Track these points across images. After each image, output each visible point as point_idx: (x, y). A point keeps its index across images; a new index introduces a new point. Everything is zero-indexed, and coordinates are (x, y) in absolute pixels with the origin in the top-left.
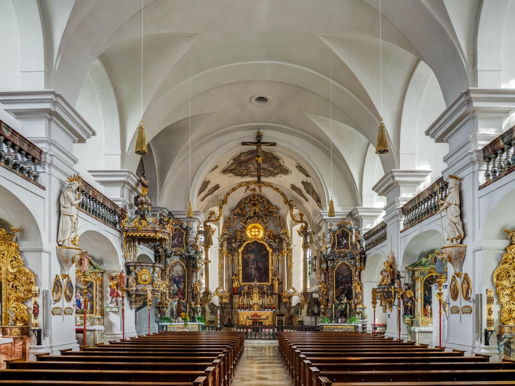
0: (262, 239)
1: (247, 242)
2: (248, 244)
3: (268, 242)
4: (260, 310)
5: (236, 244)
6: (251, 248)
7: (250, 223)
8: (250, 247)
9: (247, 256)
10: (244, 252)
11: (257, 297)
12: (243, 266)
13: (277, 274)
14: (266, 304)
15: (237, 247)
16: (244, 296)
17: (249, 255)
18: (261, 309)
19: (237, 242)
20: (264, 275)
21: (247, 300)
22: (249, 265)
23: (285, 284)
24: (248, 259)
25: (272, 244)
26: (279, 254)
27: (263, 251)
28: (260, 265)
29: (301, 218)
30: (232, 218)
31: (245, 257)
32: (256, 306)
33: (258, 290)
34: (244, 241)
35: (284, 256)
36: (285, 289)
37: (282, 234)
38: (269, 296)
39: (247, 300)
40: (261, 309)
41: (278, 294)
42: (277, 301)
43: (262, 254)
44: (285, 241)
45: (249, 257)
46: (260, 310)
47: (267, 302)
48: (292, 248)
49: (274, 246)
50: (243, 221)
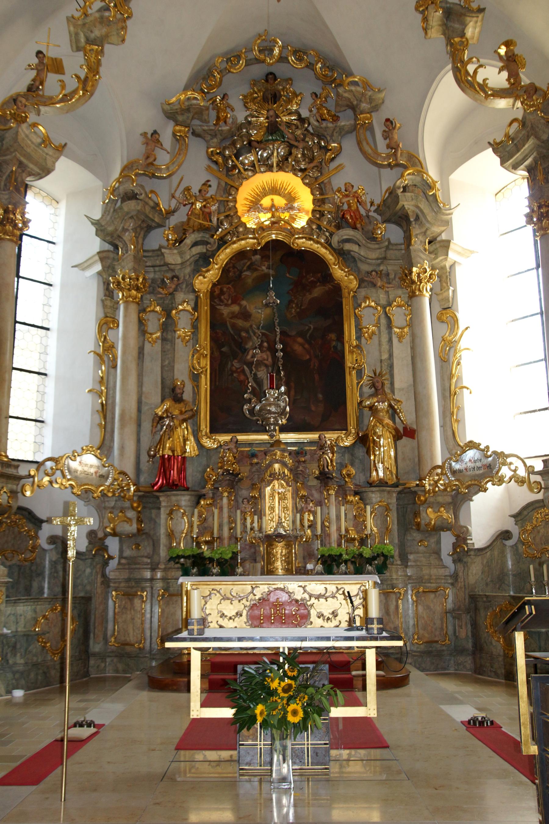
0: (307, 233)
1: (236, 246)
2: (241, 255)
3: (335, 240)
4: (306, 572)
5: (181, 254)
6: (255, 274)
7: (253, 168)
8: (249, 268)
9: (235, 308)
10: (222, 292)
11: (282, 498)
12: (217, 354)
13: (387, 390)
14: (334, 536)
15: (188, 270)
16: (216, 496)
17: (244, 303)
18: (309, 566)
19: (188, 241)
20: (320, 396)
21: (232, 521)
22: (245, 351)
23: (431, 430)
24: (240, 323)
25: (355, 248)
26: (391, 297)
27: (313, 285)
28: (298, 348)
29: (513, 76)
30: (167, 139)
31: (225, 311)
32: (279, 549)
33: (289, 461)
34: (223, 242)
35: (421, 295)
36: (432, 457)
37: (405, 189)
38: (350, 498)
39: (232, 521)
40: (309, 566)
41: (396, 485)
42: (392, 519)
43: (309, 297)
44: (421, 225)
45: (246, 315)
46: (302, 572)
47: (339, 529)
48: (452, 266)
49: (365, 260)
50: (220, 160)
